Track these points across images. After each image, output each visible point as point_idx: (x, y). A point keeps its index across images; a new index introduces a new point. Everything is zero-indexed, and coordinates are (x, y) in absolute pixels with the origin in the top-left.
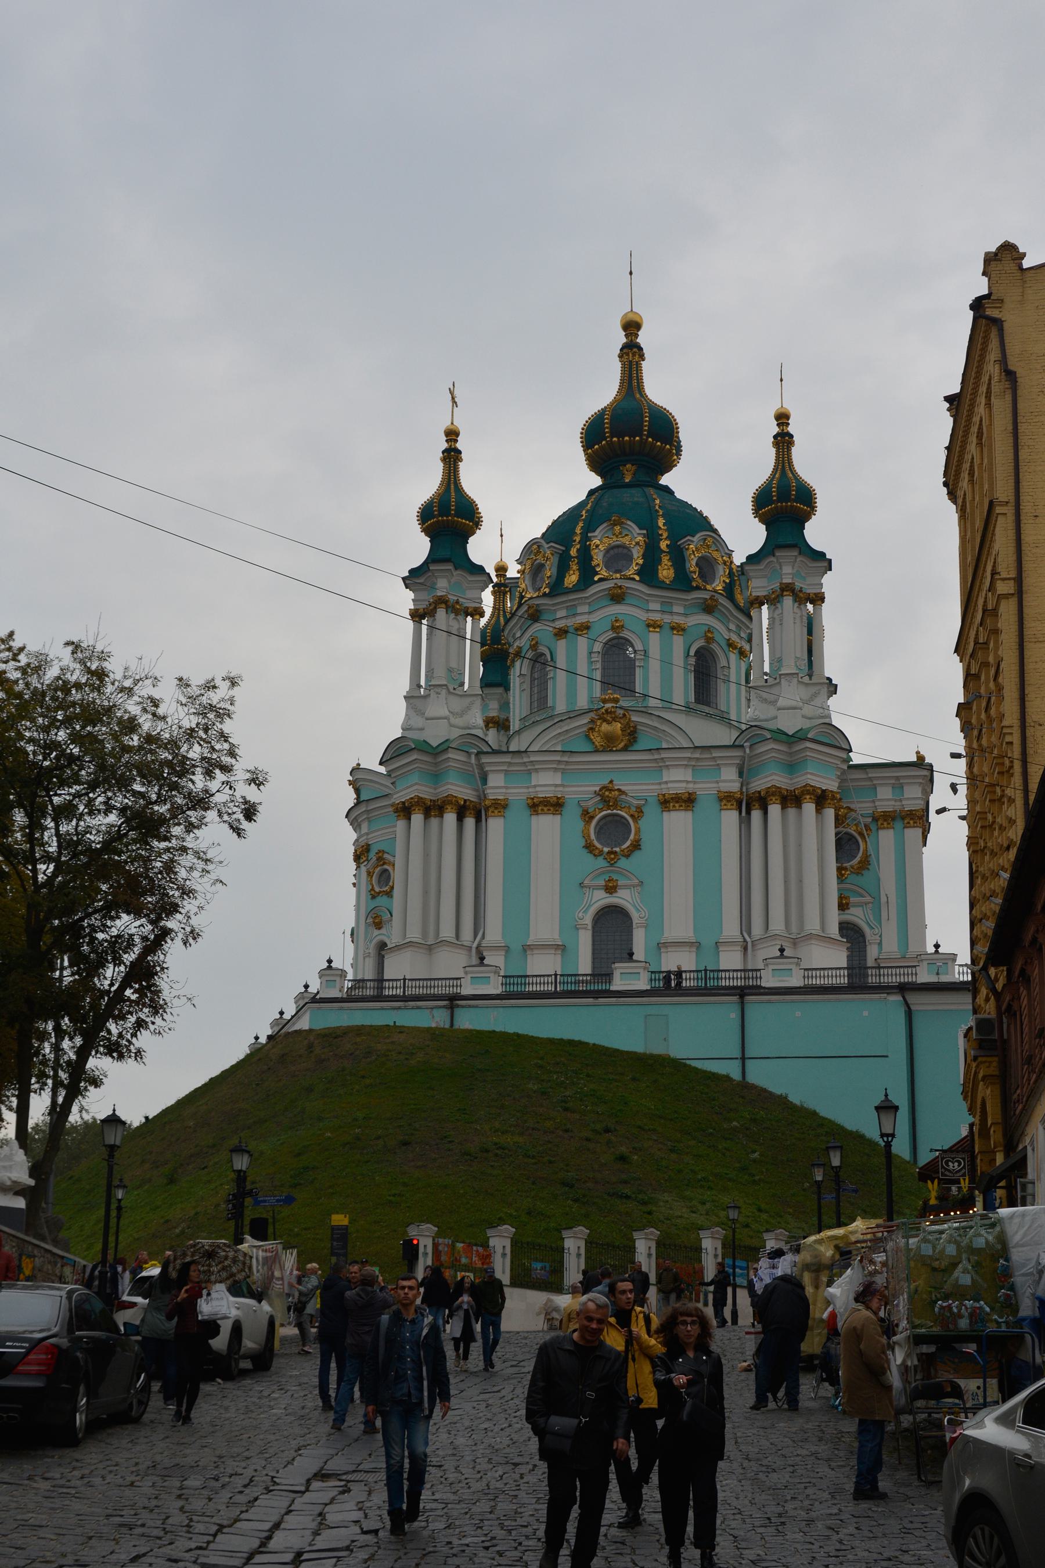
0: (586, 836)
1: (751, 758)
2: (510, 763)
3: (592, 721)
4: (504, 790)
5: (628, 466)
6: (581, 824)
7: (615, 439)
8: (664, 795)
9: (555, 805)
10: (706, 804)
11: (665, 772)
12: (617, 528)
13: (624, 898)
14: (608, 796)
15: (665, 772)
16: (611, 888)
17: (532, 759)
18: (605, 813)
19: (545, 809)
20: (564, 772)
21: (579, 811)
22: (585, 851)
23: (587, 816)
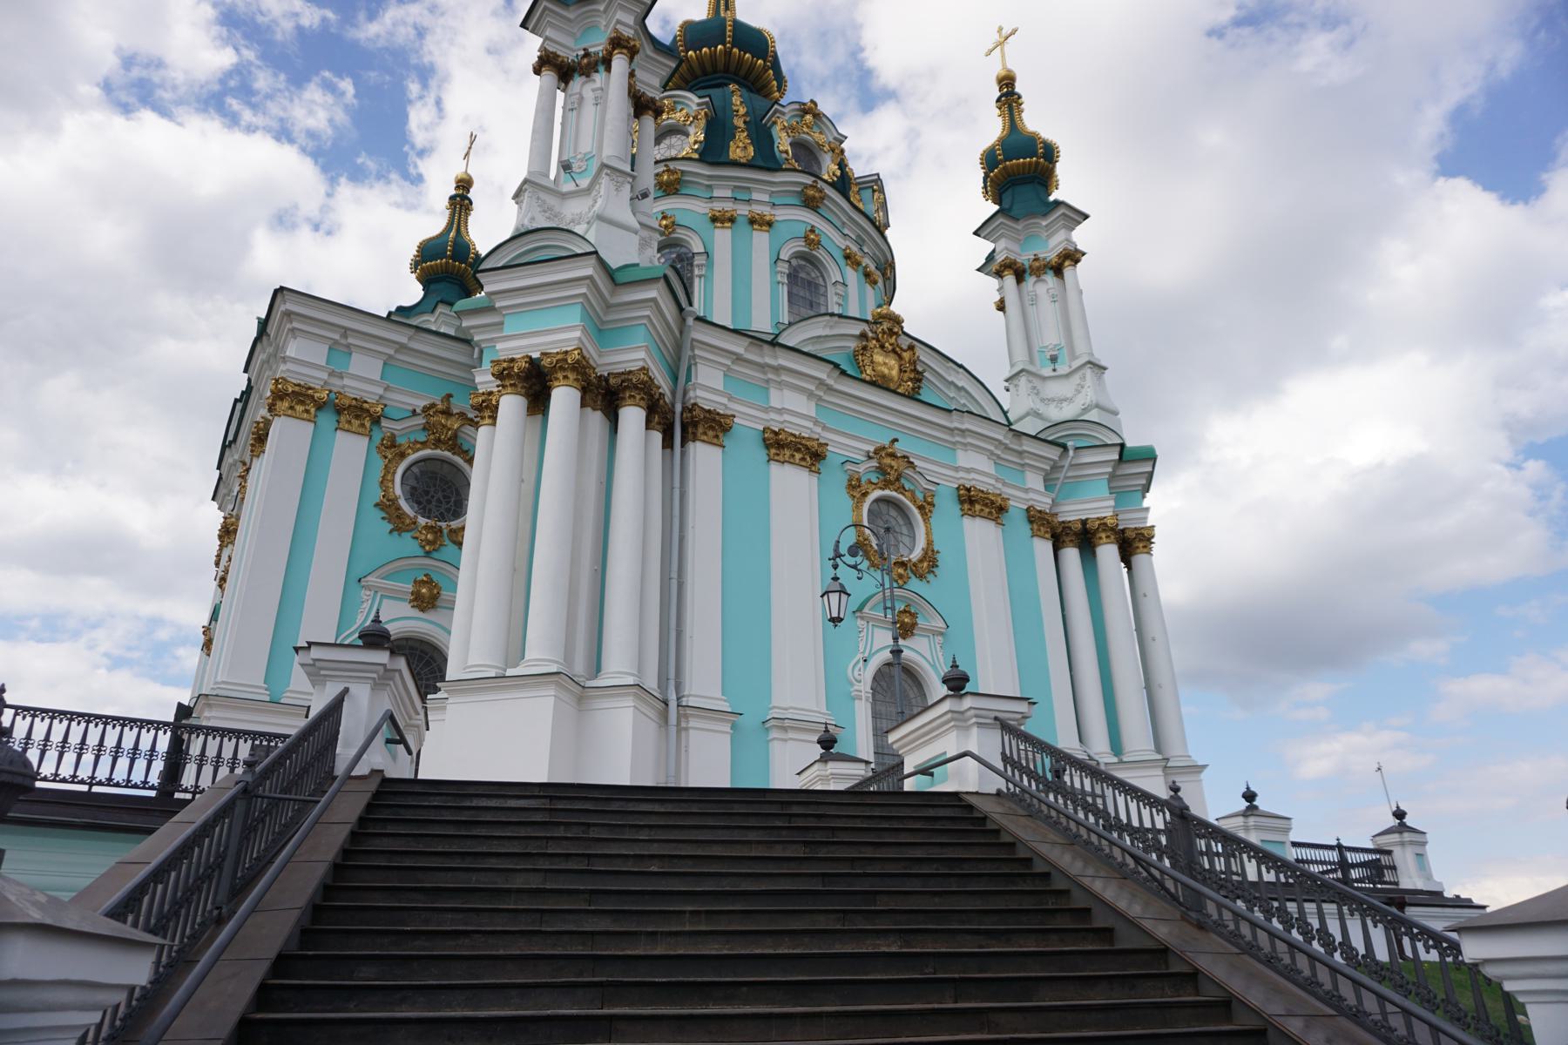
2: (738, 359)
3: (863, 336)
4: (725, 400)
6: (850, 503)
8: (969, 490)
9: (812, 455)
11: (960, 453)
12: (809, 117)
14: (890, 466)
15: (960, 453)
16: (905, 628)
17: (782, 362)
19: (798, 456)
21: (845, 478)
23: (855, 487)
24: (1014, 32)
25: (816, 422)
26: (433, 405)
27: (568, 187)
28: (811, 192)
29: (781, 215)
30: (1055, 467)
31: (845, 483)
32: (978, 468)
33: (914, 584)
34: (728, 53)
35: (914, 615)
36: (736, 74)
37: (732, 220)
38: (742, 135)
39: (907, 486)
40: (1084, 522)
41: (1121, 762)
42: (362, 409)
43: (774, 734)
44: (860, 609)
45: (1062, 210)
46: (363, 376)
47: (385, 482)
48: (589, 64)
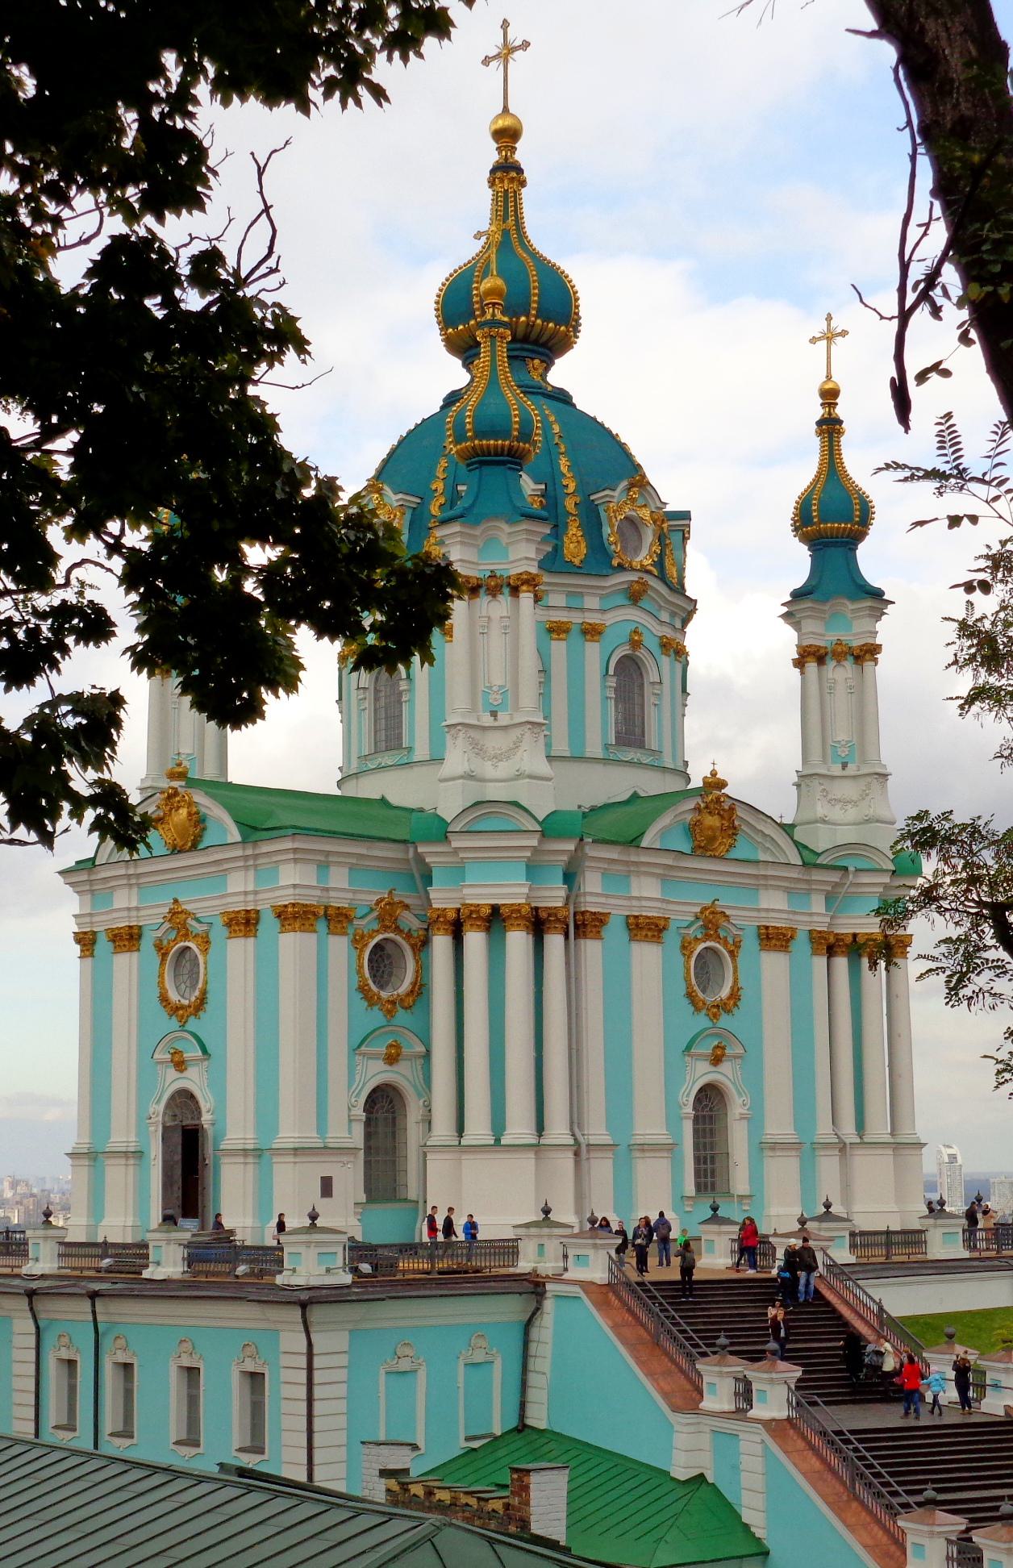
0: (687, 979)
1: (852, 884)
3: (697, 809)
4: (603, 900)
5: (537, 362)
7: (539, 321)
8: (767, 928)
10: (801, 944)
12: (635, 493)
13: (725, 1075)
14: (712, 921)
17: (643, 859)
18: (703, 946)
20: (663, 879)
22: (686, 1001)
23: (686, 947)
24: (844, 333)
25: (663, 901)
26: (382, 900)
27: (487, 720)
28: (636, 587)
29: (609, 619)
30: (836, 885)
31: (679, 944)
32: (774, 906)
33: (725, 1021)
34: (530, 326)
35: (724, 1048)
36: (536, 342)
37: (567, 631)
38: (573, 530)
39: (722, 934)
40: (855, 935)
41: (863, 1144)
42: (341, 914)
43: (638, 1154)
44: (688, 1048)
45: (869, 603)
46: (340, 886)
47: (360, 971)
48: (496, 586)
